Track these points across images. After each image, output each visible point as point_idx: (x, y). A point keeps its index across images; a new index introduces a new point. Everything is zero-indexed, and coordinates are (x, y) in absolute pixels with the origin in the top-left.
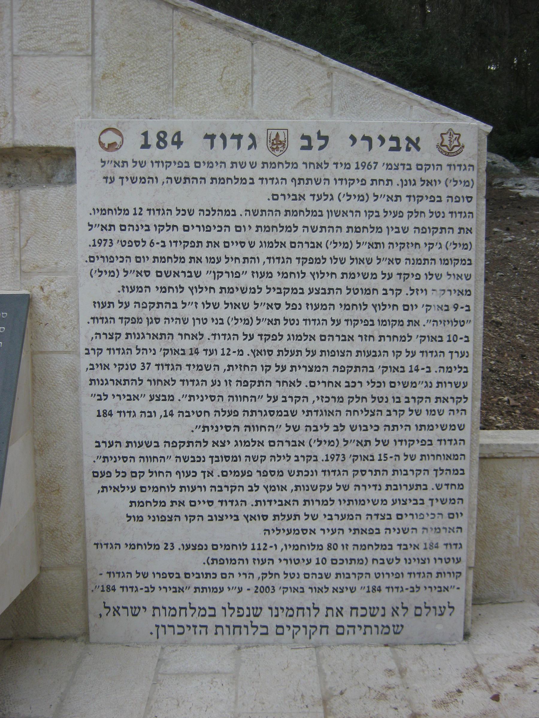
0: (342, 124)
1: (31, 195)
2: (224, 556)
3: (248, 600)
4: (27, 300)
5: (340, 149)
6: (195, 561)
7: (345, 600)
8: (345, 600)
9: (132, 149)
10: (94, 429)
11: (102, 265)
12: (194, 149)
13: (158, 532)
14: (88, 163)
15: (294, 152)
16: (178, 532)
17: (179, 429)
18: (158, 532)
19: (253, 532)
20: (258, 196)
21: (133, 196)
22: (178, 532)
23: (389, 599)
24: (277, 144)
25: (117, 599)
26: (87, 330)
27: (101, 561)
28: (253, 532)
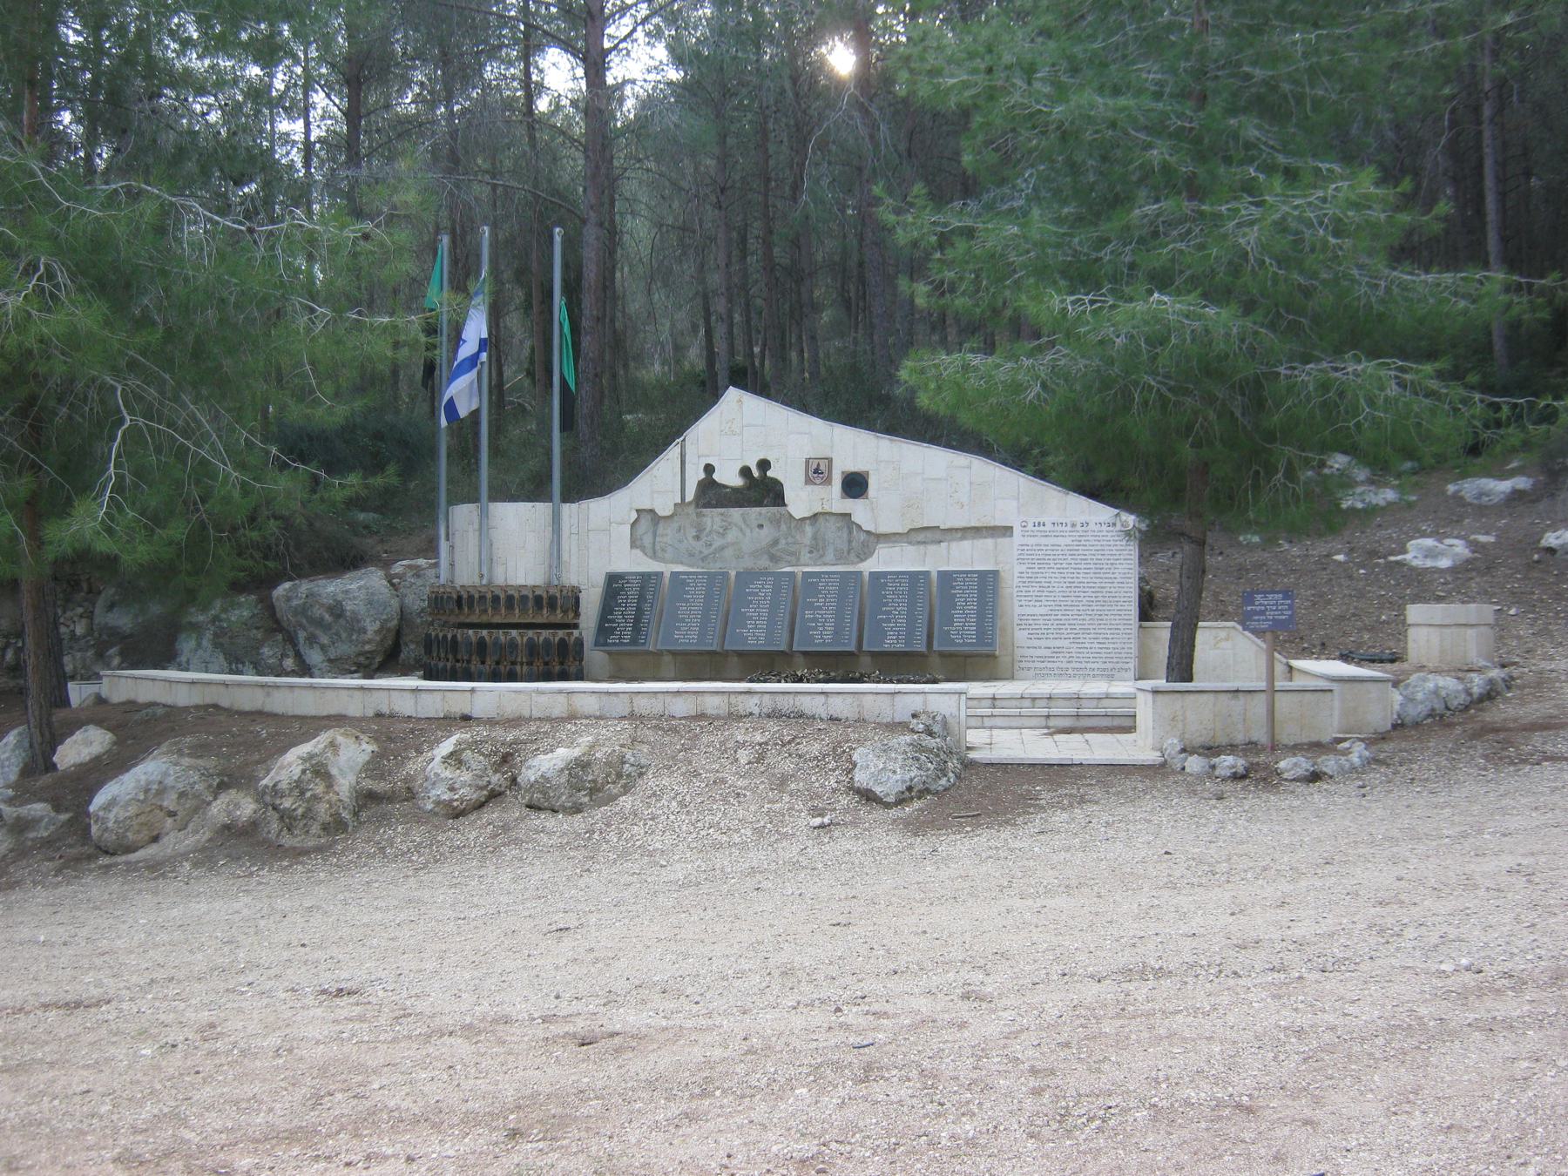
0: (1093, 519)
1: (1000, 540)
2: (1057, 651)
3: (1064, 665)
4: (995, 573)
5: (1092, 526)
6: (1047, 653)
7: (1095, 666)
8: (1095, 666)
9: (1030, 527)
10: (1018, 610)
11: (1021, 561)
12: (1049, 527)
13: (1037, 643)
14: (1017, 531)
15: (1078, 527)
16: (1043, 643)
17: (1043, 611)
18: (1037, 643)
19: (1066, 643)
20: (1068, 541)
21: (1031, 541)
22: (1043, 643)
23: (1109, 666)
24: (1073, 525)
25: (1023, 665)
26: (1016, 580)
27: (1018, 652)
28: (1066, 643)
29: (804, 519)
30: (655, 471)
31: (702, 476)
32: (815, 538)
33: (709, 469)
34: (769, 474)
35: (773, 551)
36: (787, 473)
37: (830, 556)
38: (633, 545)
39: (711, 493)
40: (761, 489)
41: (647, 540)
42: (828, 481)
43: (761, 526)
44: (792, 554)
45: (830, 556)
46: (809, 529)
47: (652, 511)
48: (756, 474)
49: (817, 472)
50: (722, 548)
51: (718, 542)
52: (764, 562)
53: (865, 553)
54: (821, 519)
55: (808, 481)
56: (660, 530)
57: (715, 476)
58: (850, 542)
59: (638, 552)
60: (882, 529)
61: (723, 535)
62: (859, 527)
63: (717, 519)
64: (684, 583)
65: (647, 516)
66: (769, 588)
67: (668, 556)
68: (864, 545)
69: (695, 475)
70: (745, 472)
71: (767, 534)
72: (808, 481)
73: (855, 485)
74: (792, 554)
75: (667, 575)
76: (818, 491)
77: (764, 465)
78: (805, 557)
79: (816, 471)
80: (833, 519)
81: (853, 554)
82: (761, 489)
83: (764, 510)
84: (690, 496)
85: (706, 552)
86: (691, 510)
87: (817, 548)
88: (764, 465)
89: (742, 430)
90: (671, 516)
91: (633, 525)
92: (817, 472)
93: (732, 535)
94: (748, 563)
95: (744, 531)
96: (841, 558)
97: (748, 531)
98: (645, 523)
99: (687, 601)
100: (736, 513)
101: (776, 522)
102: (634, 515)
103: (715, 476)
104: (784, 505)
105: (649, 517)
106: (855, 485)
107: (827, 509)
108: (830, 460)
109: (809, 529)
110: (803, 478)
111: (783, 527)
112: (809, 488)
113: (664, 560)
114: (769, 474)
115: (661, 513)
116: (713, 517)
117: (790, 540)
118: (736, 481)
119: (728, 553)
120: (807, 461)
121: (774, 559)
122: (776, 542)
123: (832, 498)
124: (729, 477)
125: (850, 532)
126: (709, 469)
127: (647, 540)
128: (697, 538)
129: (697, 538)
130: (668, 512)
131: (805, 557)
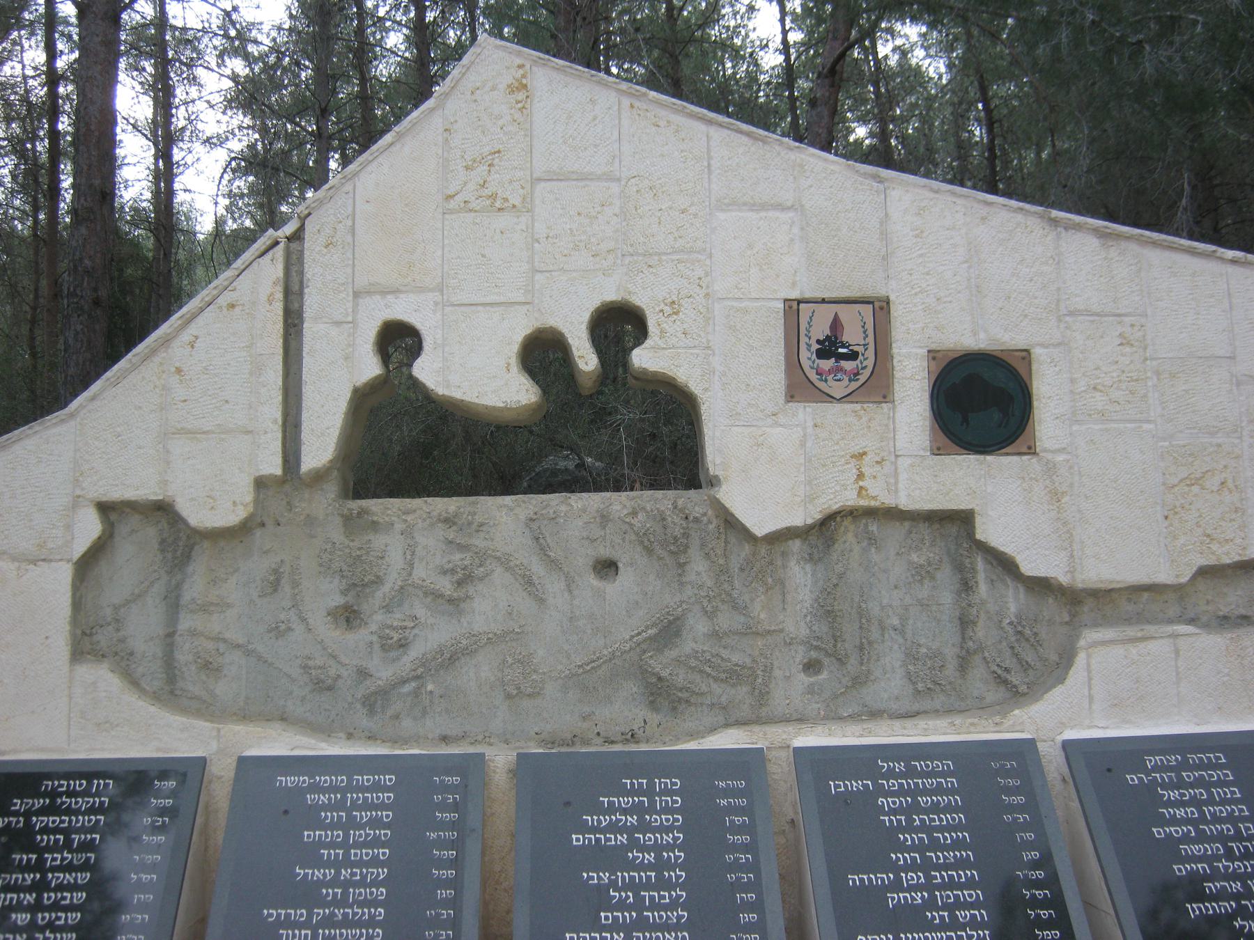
29: (779, 537)
30: (178, 351)
31: (370, 368)
32: (826, 611)
33: (399, 341)
34: (642, 358)
35: (660, 664)
36: (716, 355)
37: (890, 683)
38: (85, 645)
39: (411, 443)
40: (608, 421)
41: (142, 628)
42: (877, 386)
43: (607, 567)
44: (734, 676)
45: (890, 683)
46: (801, 579)
47: (162, 510)
48: (586, 359)
49: (832, 351)
50: (451, 658)
51: (436, 633)
52: (624, 710)
53: (1030, 668)
54: (848, 536)
55: (800, 387)
56: (196, 585)
57: (426, 370)
58: (965, 623)
59: (103, 677)
60: (1100, 568)
61: (455, 605)
62: (1004, 564)
63: (430, 542)
64: (296, 812)
65: (145, 527)
66: (668, 829)
67: (223, 689)
68: (1022, 632)
69: (342, 366)
70: (543, 354)
71: (630, 600)
72: (800, 387)
73: (983, 402)
74: (734, 676)
75: (223, 770)
76: (837, 424)
77: (619, 325)
78: (791, 686)
79: (829, 348)
80: (895, 533)
81: (978, 672)
82: (608, 421)
83: (618, 502)
84: (320, 448)
85: (384, 673)
86: (325, 503)
87: (838, 650)
88: (619, 325)
89: (522, 208)
90: (242, 531)
91: (87, 564)
92: (832, 351)
93: (490, 606)
94: (557, 716)
95: (538, 583)
96: (932, 689)
97: (554, 587)
98: (134, 559)
99: (308, 895)
100: (505, 517)
101: (669, 549)
102: (89, 527)
103: (426, 370)
104: (714, 482)
105: (151, 533)
106: (983, 402)
107: (879, 494)
108: (881, 308)
109: (801, 579)
110: (777, 378)
111: (698, 567)
112: (805, 413)
113: (206, 709)
114: (642, 358)
115: (198, 515)
116: (413, 530)
117: (726, 620)
118: (504, 389)
119: (477, 673)
120: (793, 308)
121: (660, 694)
122: (669, 630)
123: (900, 452)
124: (477, 372)
125: (967, 586)
126: (399, 341)
127: (142, 628)
128: (348, 616)
129: (348, 616)
130: (227, 515)
131: (791, 686)
